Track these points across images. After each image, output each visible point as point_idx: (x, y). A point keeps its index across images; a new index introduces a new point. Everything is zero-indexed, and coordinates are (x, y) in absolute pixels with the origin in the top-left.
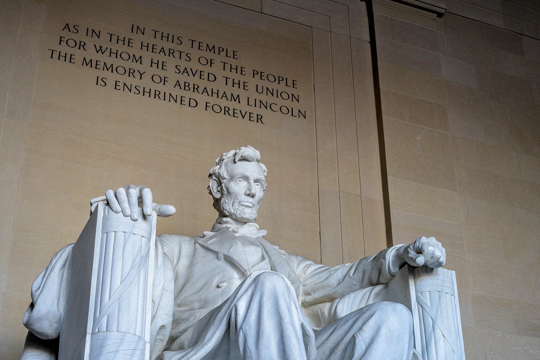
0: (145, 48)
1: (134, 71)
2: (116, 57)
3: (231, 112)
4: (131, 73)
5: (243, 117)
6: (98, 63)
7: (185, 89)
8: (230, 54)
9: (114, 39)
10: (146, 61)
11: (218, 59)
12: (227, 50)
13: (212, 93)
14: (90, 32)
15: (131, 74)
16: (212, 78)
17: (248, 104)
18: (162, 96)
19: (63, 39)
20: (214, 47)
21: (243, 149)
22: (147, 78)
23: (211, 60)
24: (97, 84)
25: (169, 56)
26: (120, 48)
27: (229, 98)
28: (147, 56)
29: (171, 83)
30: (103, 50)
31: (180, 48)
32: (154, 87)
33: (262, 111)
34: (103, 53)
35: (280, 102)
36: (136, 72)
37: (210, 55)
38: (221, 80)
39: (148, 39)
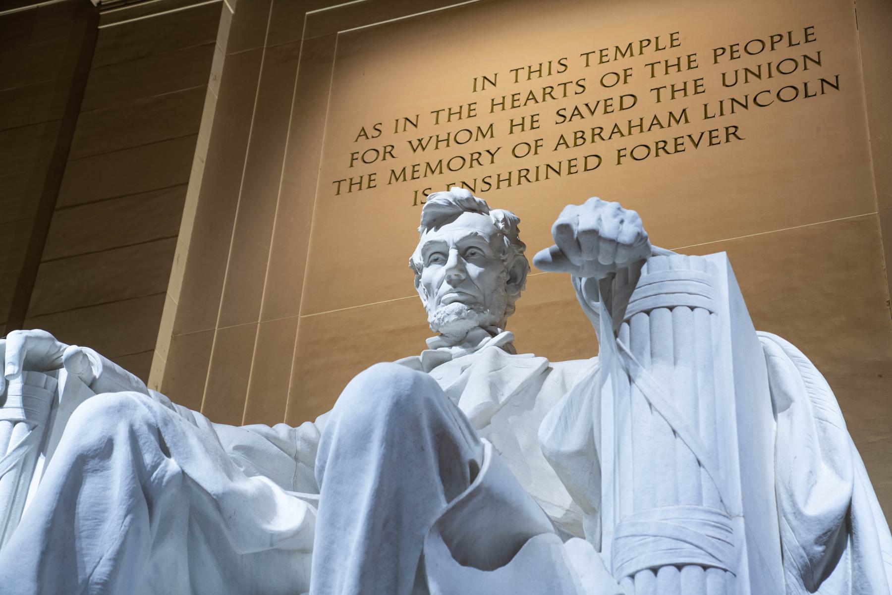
0: (497, 108)
2: (448, 146)
3: (670, 147)
4: (476, 158)
5: (696, 145)
7: (576, 145)
8: (665, 42)
9: (444, 116)
10: (501, 128)
11: (637, 63)
13: (630, 127)
15: (475, 162)
16: (628, 101)
17: (706, 117)
18: (532, 176)
23: (625, 70)
24: (415, 204)
25: (544, 100)
26: (455, 125)
27: (665, 123)
29: (549, 143)
30: (424, 143)
31: (563, 78)
32: (516, 165)
33: (740, 117)
34: (424, 149)
35: (778, 81)
38: (646, 98)
39: (506, 87)
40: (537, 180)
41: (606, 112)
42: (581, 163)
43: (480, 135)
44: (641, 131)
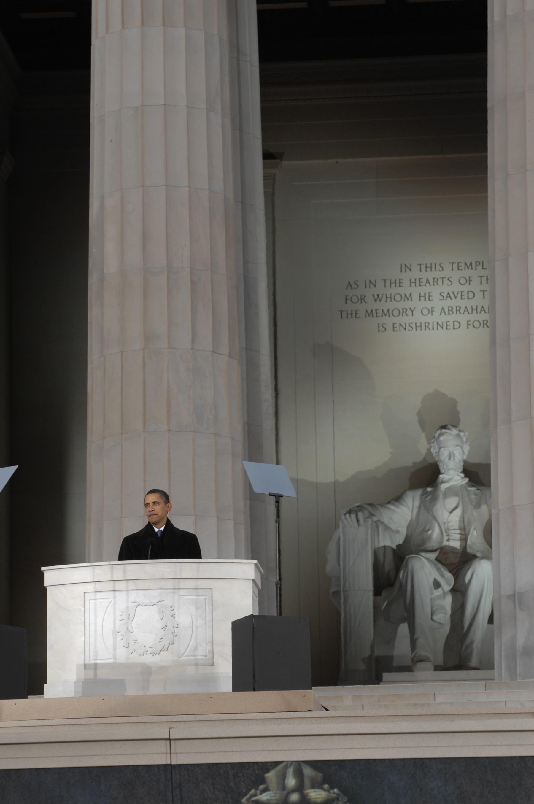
0: (413, 285)
1: (407, 310)
4: (403, 312)
6: (378, 311)
7: (449, 314)
10: (415, 297)
12: (483, 262)
13: (472, 310)
14: (368, 283)
16: (471, 295)
18: (430, 326)
19: (348, 298)
20: (471, 263)
21: (443, 430)
22: (417, 313)
23: (470, 277)
24: (379, 331)
25: (434, 285)
28: (415, 291)
29: (437, 311)
30: (380, 297)
31: (442, 274)
34: (380, 301)
36: (409, 310)
37: (467, 273)
38: (479, 295)
40: (433, 329)
41: (462, 299)
42: (451, 324)
43: (406, 299)
44: (477, 313)
